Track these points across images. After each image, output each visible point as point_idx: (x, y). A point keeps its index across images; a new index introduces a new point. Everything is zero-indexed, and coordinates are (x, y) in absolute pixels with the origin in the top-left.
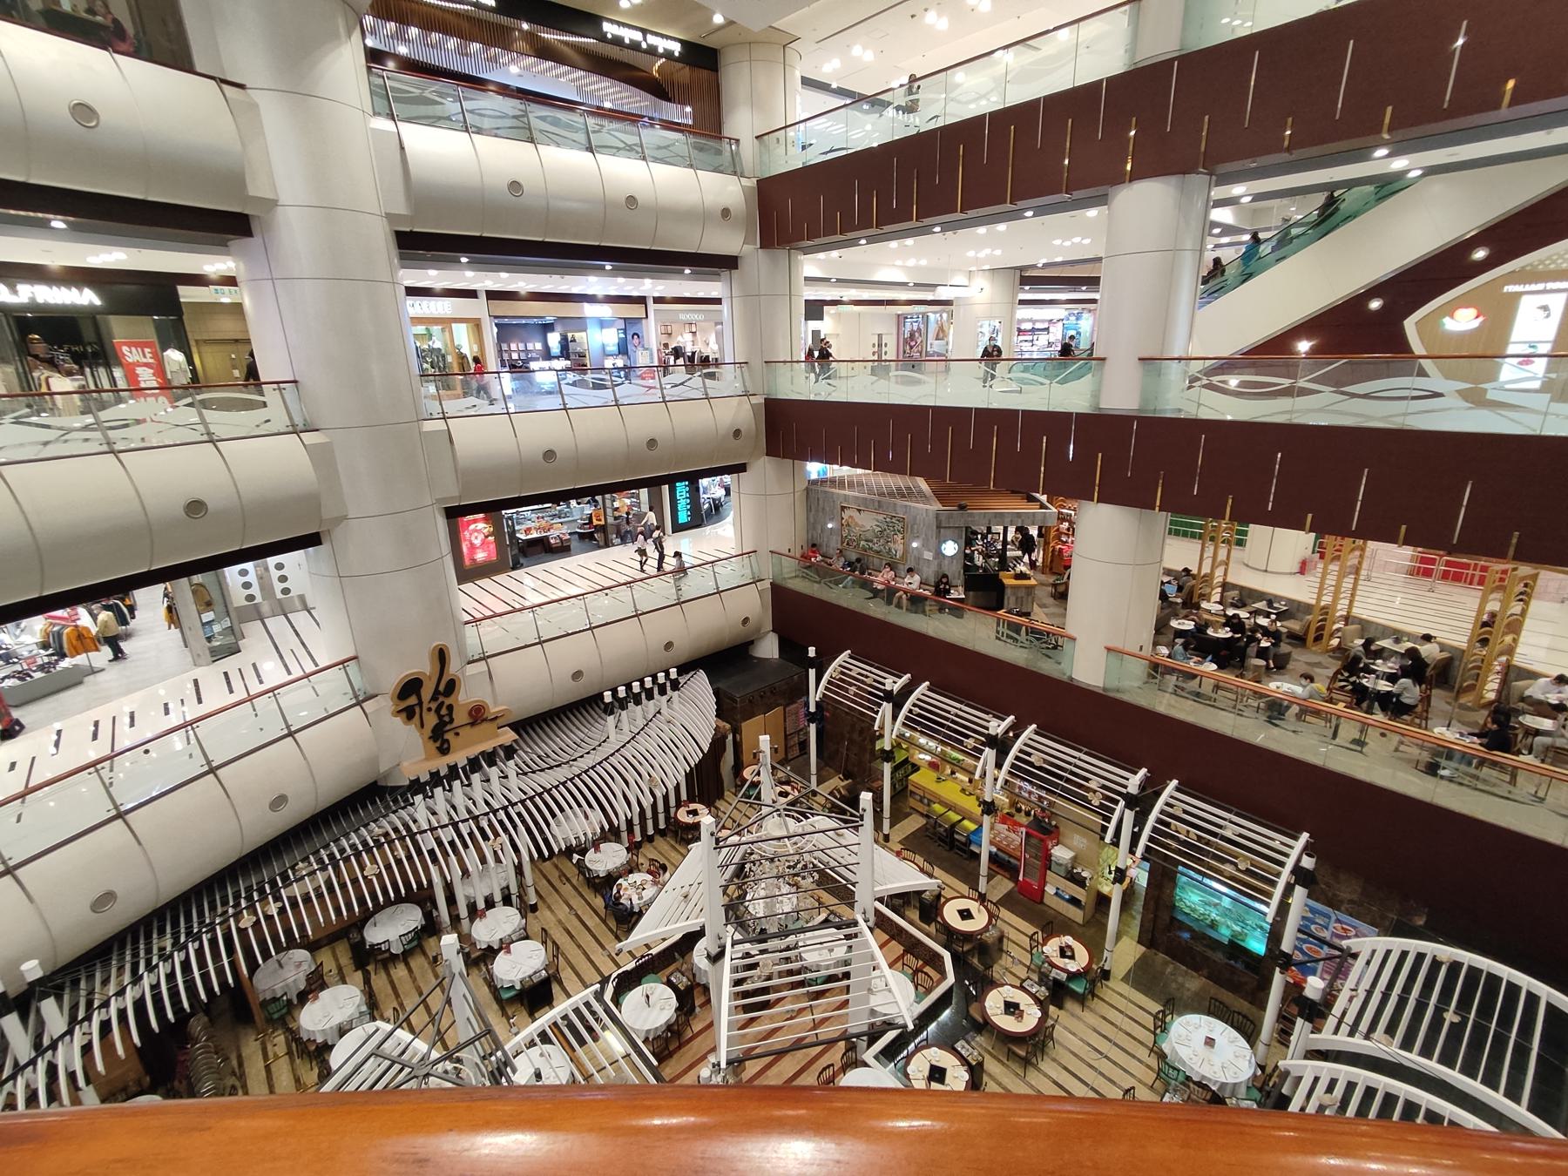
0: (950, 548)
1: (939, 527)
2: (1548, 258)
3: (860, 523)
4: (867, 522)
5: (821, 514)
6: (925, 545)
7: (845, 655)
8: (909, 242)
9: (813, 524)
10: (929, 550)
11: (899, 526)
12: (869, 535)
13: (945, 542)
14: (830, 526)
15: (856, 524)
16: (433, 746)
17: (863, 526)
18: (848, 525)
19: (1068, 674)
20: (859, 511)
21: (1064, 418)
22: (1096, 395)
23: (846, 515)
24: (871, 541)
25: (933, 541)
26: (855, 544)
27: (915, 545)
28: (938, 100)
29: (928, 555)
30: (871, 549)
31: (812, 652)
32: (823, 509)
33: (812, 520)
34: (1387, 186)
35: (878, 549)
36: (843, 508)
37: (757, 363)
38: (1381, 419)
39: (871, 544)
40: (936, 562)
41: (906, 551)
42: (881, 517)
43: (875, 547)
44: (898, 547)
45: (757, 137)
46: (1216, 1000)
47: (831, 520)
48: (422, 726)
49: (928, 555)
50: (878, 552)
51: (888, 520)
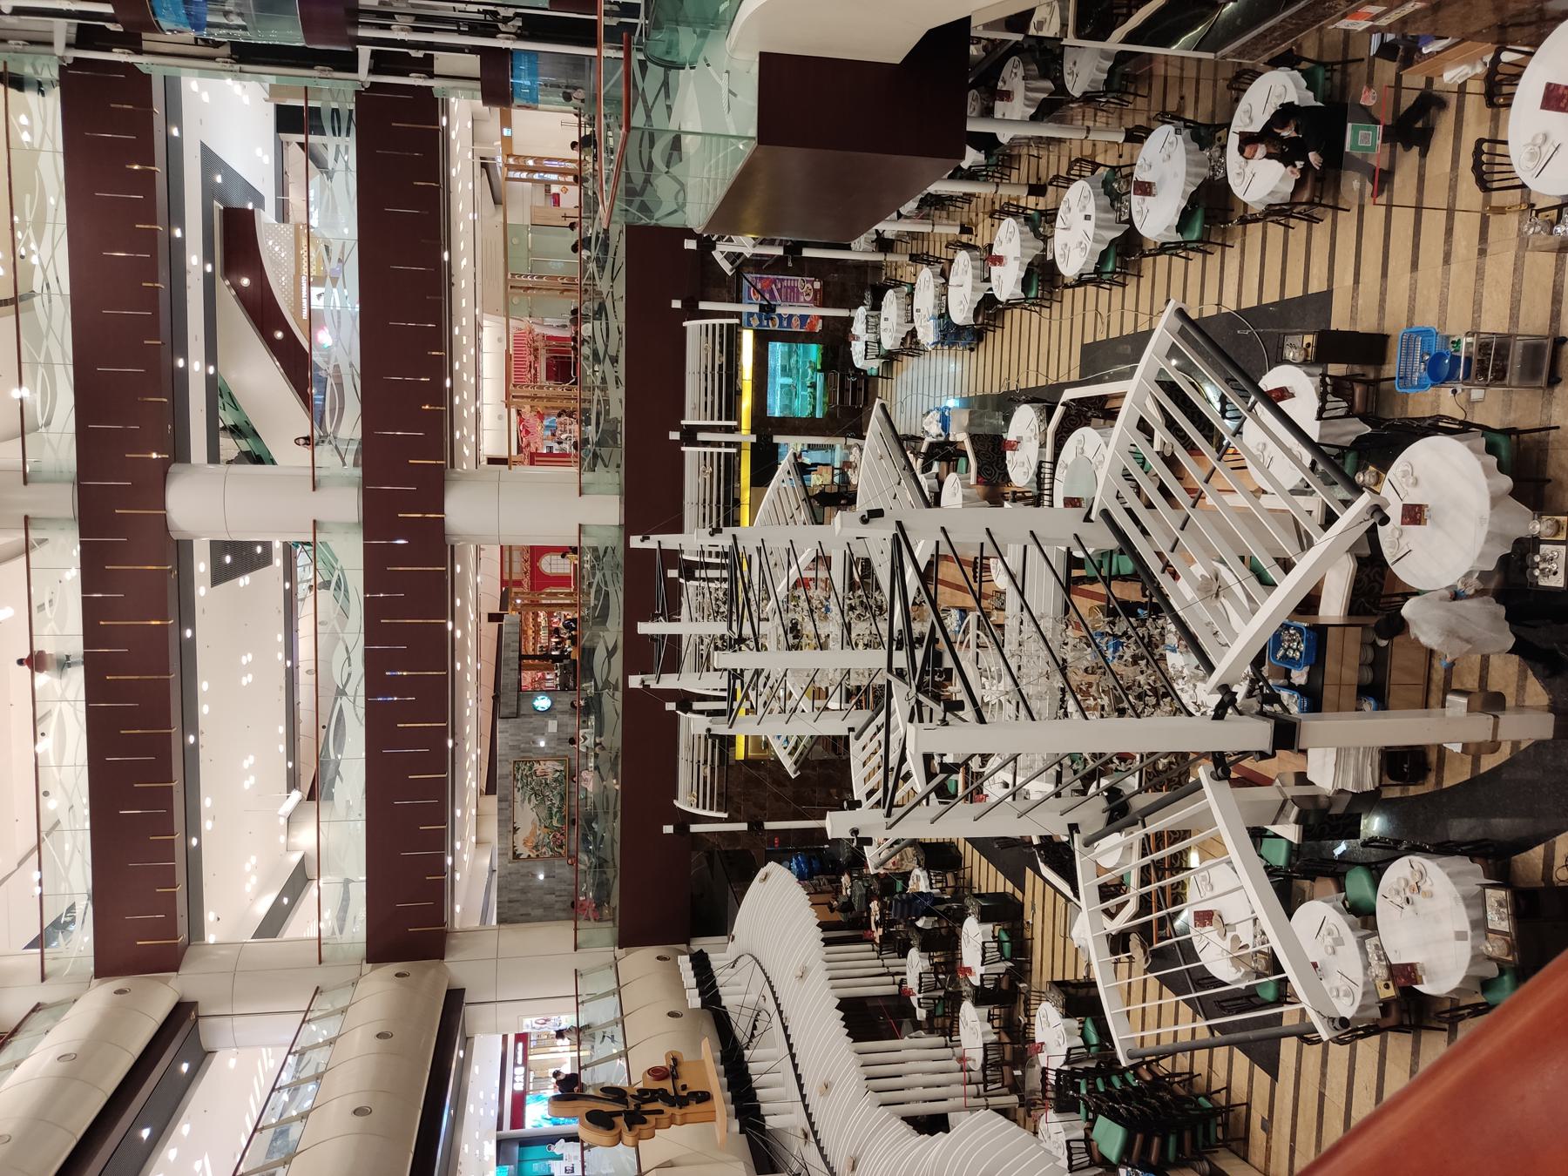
0: (542, 703)
1: (517, 715)
2: (283, 293)
3: (530, 828)
4: (527, 816)
5: (530, 895)
6: (541, 731)
7: (677, 804)
8: (206, 802)
9: (548, 914)
10: (546, 725)
11: (525, 768)
12: (544, 814)
13: (535, 709)
14: (541, 877)
15: (533, 833)
16: (694, 1107)
17: (533, 823)
18: (536, 847)
19: (617, 530)
20: (515, 830)
21: (368, 551)
22: (347, 527)
23: (524, 851)
24: (550, 809)
25: (536, 721)
26: (558, 835)
27: (542, 744)
28: (60, 710)
29: (552, 726)
30: (560, 808)
31: (668, 829)
32: (523, 891)
33: (539, 912)
34: (216, 390)
35: (558, 798)
36: (516, 856)
37: (320, 976)
38: (354, 321)
39: (555, 810)
40: (559, 716)
41: (555, 758)
42: (518, 796)
43: (557, 803)
44: (550, 768)
45: (43, 979)
46: (866, 355)
47: (534, 876)
48: (661, 1112)
49: (552, 726)
50: (562, 799)
51: (519, 785)
